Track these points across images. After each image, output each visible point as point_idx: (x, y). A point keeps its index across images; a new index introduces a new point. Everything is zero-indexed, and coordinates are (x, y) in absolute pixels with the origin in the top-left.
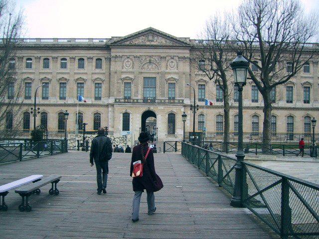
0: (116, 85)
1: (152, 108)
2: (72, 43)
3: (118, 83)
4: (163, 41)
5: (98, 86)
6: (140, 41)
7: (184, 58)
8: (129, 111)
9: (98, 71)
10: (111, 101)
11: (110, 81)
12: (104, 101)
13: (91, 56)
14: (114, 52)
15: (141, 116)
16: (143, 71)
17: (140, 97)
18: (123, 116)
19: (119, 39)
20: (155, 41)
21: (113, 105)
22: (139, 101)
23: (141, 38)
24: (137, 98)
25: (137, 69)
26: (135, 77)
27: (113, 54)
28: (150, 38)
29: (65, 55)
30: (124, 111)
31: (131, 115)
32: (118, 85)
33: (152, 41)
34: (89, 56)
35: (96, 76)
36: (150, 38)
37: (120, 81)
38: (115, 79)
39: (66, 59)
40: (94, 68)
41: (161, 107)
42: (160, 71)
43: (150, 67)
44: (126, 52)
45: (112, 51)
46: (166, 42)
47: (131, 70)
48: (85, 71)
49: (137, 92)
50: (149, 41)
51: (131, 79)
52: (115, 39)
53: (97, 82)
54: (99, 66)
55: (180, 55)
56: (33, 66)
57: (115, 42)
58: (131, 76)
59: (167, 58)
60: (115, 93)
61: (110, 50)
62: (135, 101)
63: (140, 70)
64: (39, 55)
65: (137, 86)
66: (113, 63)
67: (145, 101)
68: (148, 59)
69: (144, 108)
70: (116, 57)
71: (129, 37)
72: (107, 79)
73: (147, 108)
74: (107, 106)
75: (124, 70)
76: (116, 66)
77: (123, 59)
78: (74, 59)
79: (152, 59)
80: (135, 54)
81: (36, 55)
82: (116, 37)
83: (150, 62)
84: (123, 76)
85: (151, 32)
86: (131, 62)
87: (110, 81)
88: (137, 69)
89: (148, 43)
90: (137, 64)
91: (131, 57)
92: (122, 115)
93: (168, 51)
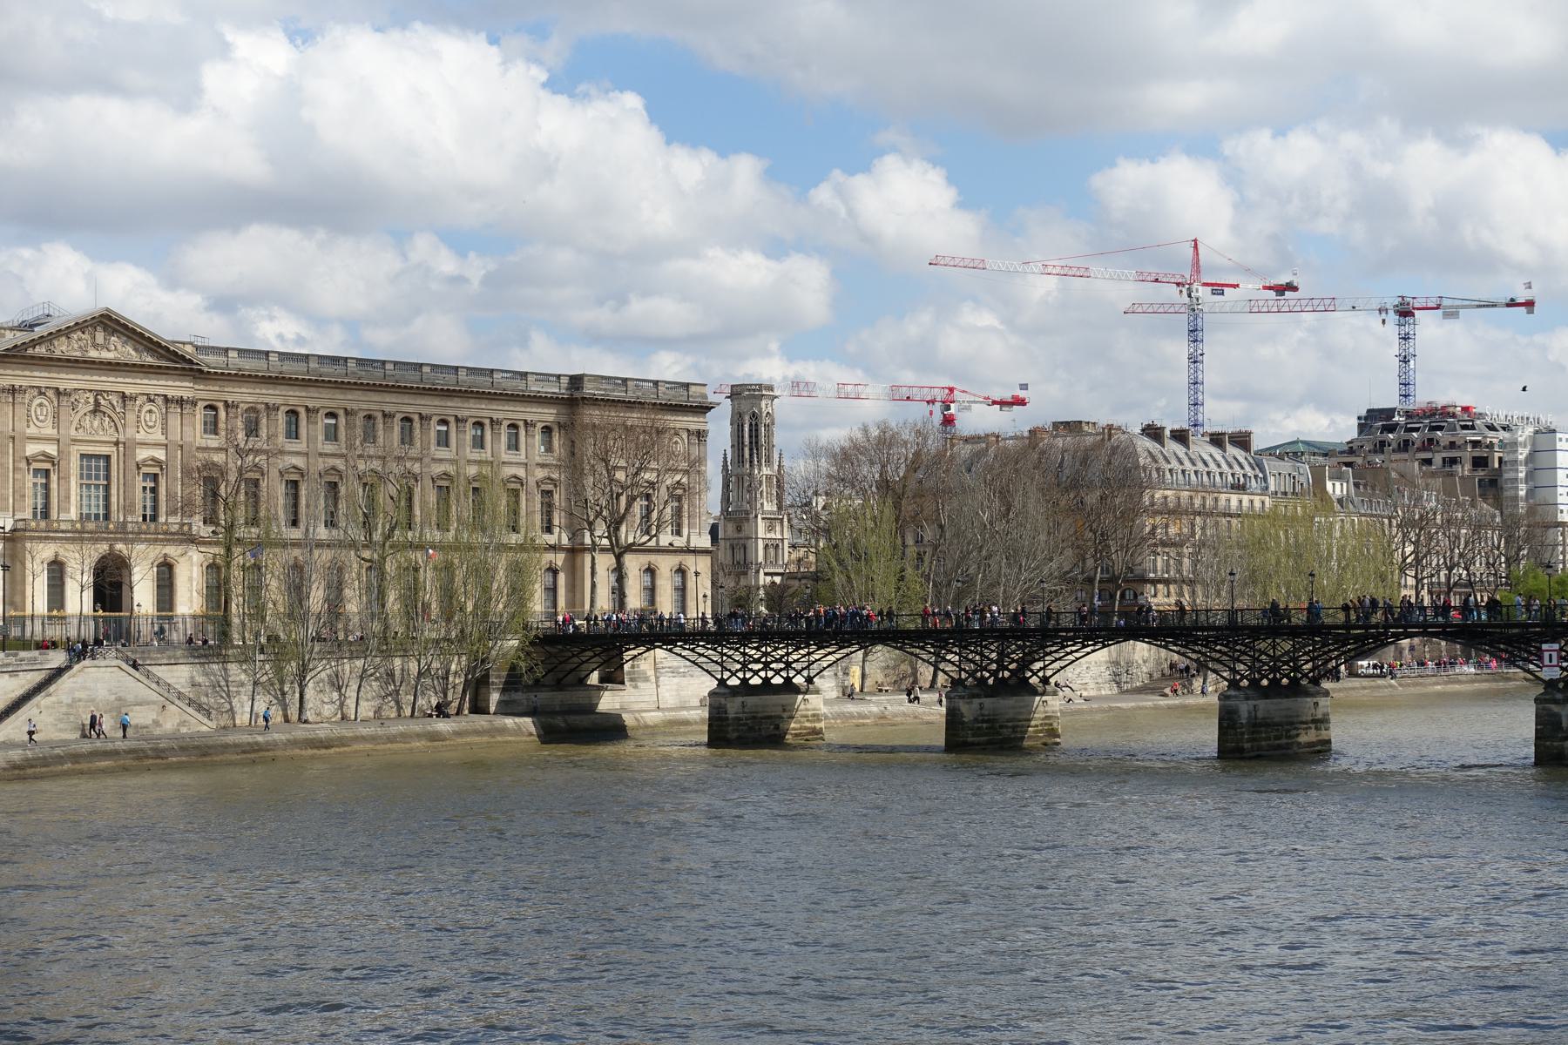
7: (181, 402)
16: (81, 435)
28: (100, 337)
41: (141, 547)
42: (122, 439)
44: (40, 377)
49: (68, 497)
50: (95, 346)
51: (48, 458)
55: (170, 393)
58: (52, 450)
63: (73, 432)
65: (67, 479)
73: (106, 547)
83: (97, 410)
84: (32, 449)
89: (93, 354)
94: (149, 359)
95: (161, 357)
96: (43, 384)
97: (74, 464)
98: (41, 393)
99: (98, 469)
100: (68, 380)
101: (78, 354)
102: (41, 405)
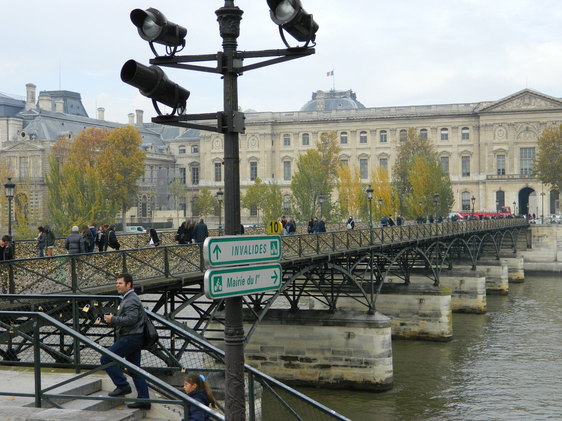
0: (487, 159)
1: (531, 185)
2: (433, 110)
3: (489, 156)
4: (543, 104)
5: (466, 160)
6: (515, 106)
8: (503, 189)
9: (465, 142)
10: (482, 177)
11: (479, 153)
12: (474, 177)
13: (456, 125)
14: (484, 120)
15: (518, 194)
16: (519, 140)
17: (516, 171)
18: (497, 195)
19: (489, 105)
20: (533, 104)
21: (484, 183)
22: (515, 177)
23: (515, 101)
24: (512, 173)
25: (511, 138)
26: (509, 148)
27: (482, 123)
28: (527, 101)
29: (425, 125)
30: (498, 189)
31: (505, 193)
32: (490, 159)
33: (529, 104)
34: (453, 125)
35: (462, 149)
36: (527, 101)
37: (492, 154)
38: (486, 152)
39: (426, 130)
40: (460, 139)
43: (527, 135)
44: (498, 119)
45: (481, 119)
46: (546, 104)
47: (504, 140)
48: (450, 143)
49: (512, 166)
50: (525, 104)
51: (505, 151)
52: (485, 105)
53: (463, 155)
54: (465, 137)
56: (389, 140)
57: (484, 109)
58: (505, 147)
59: (548, 125)
60: (487, 168)
61: (479, 116)
62: (511, 177)
63: (516, 140)
64: (395, 127)
65: (512, 158)
66: (482, 133)
67: (522, 177)
68: (525, 126)
69: (522, 185)
70: (486, 126)
71: (501, 102)
72: (476, 152)
74: (478, 183)
75: (497, 140)
76: (486, 137)
77: (494, 128)
78: (436, 129)
79: (530, 126)
80: (509, 122)
81: (391, 127)
82: (485, 102)
83: (527, 129)
84: (496, 148)
85: (527, 94)
86: (505, 131)
87: (479, 153)
88: (511, 138)
89: (524, 108)
90: (511, 133)
91: (503, 125)
92: (495, 194)
93: (548, 115)
94: (552, 107)
95: (559, 105)
96: (500, 122)
97: (517, 152)
98: (500, 126)
99: (530, 153)
100: (512, 119)
101: (516, 108)
102: (501, 130)
